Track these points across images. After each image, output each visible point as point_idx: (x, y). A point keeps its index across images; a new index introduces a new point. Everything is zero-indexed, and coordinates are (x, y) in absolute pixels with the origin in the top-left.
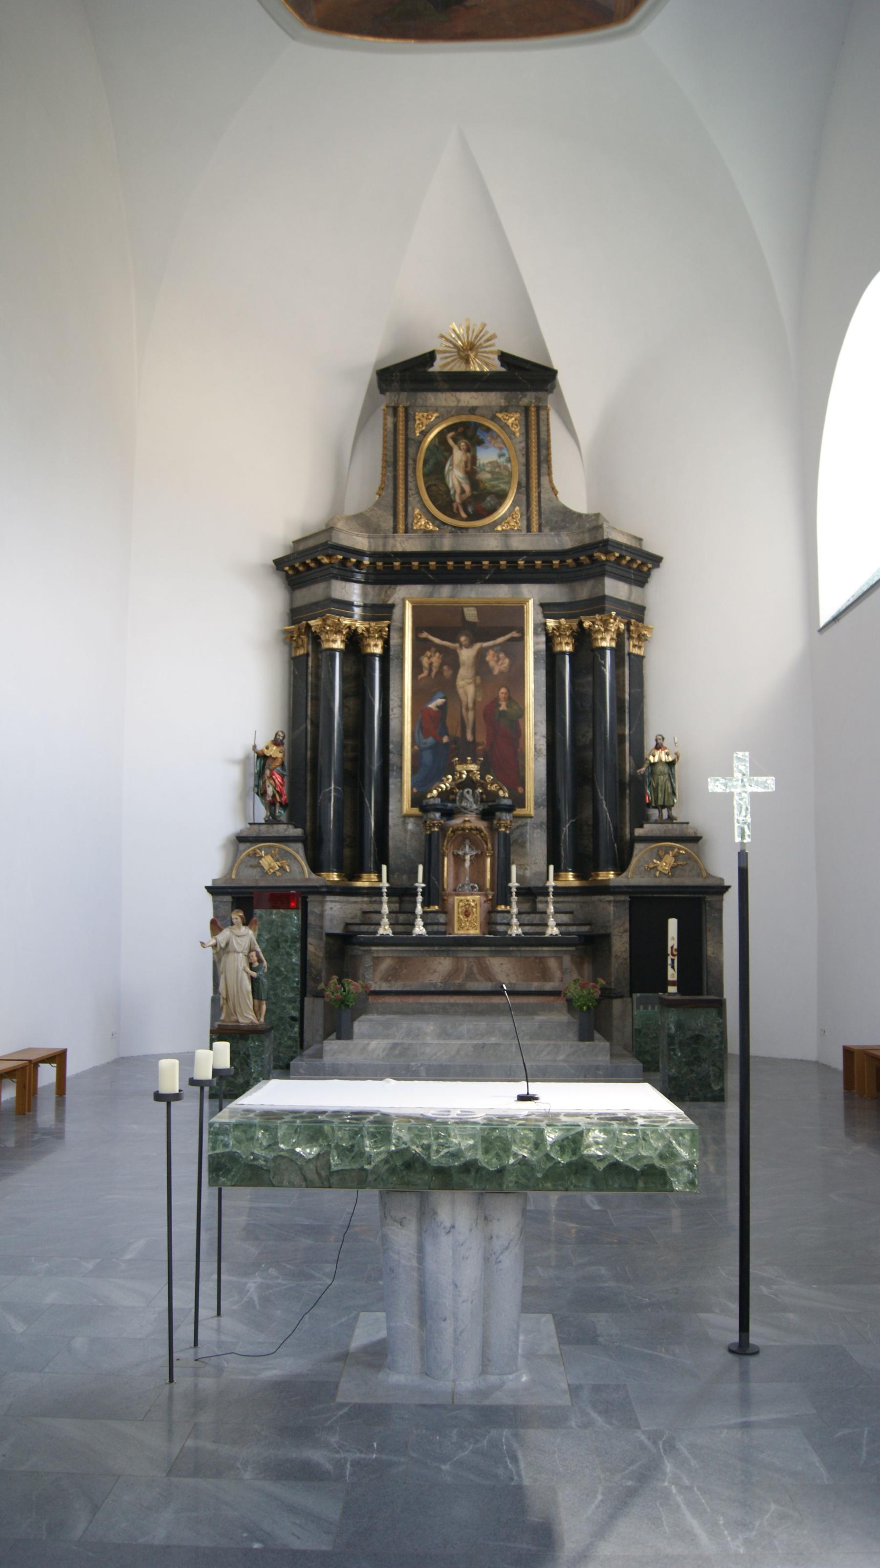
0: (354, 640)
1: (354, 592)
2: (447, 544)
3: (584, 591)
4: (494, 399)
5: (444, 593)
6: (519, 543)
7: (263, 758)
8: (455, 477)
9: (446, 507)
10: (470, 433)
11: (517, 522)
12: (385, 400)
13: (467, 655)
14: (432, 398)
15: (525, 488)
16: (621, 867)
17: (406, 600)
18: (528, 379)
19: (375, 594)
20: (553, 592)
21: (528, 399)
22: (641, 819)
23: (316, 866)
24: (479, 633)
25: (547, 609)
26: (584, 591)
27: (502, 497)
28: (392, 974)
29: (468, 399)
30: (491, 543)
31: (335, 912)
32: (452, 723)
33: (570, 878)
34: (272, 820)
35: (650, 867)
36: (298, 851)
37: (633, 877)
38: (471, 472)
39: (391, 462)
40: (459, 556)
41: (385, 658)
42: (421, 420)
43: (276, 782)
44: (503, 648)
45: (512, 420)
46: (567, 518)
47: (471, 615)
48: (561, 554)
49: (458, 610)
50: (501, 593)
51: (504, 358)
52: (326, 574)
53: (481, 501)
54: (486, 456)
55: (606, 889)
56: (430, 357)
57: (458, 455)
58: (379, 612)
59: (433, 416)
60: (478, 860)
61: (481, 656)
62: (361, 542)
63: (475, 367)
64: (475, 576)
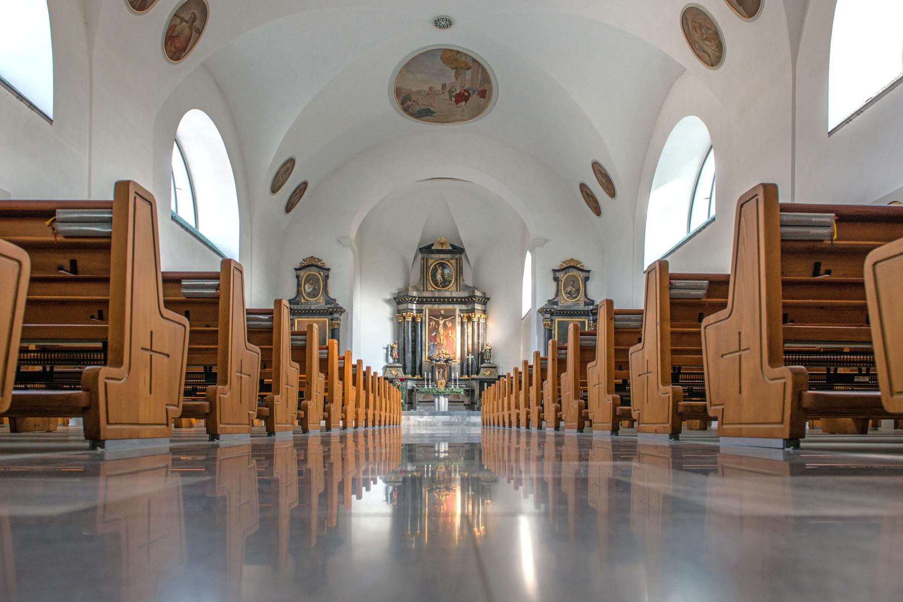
0: (414, 319)
1: (414, 307)
2: (437, 294)
3: (470, 307)
4: (449, 256)
5: (436, 306)
6: (455, 294)
7: (392, 348)
8: (439, 277)
9: (436, 284)
10: (443, 266)
11: (454, 288)
12: (420, 256)
13: (441, 322)
14: (433, 255)
15: (456, 280)
16: (478, 373)
17: (426, 308)
18: (457, 250)
19: (419, 307)
20: (464, 307)
21: (457, 256)
22: (483, 362)
23: (405, 373)
24: (444, 317)
25: (461, 311)
26: (470, 307)
27: (450, 282)
28: (424, 397)
29: (442, 256)
30: (448, 294)
31: (410, 384)
32: (438, 339)
33: (466, 377)
34: (394, 362)
35: (485, 374)
36: (401, 369)
37: (480, 376)
38: (443, 276)
39: (422, 272)
40: (439, 298)
41: (421, 323)
42: (430, 261)
43: (395, 354)
44: (450, 321)
45: (453, 261)
46: (467, 287)
47: (442, 312)
48: (465, 298)
49: (439, 310)
50: (450, 307)
51: (451, 245)
52: (407, 302)
53: (445, 283)
54: (446, 271)
55: (473, 379)
56: (433, 245)
57: (440, 271)
58: (420, 311)
59: (433, 259)
60: (444, 371)
61: (445, 323)
62: (415, 294)
63: (444, 248)
64: (444, 303)
